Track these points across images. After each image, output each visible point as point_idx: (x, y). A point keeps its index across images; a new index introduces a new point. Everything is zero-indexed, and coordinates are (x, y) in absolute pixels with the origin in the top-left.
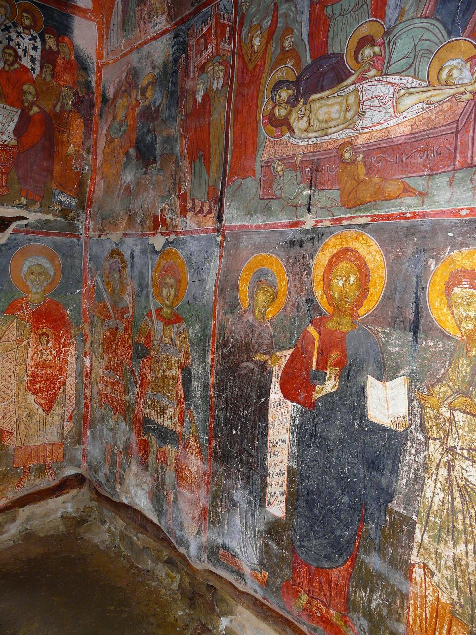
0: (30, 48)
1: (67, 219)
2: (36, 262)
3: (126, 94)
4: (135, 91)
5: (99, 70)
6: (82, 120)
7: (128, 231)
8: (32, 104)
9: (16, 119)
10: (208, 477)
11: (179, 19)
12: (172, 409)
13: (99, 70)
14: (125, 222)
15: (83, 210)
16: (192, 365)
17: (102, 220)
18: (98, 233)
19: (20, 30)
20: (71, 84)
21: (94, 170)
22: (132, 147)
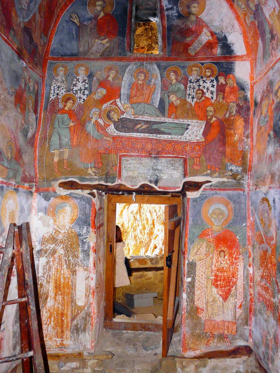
0: (210, 87)
1: (236, 180)
2: (217, 207)
3: (267, 98)
4: (271, 94)
5: (252, 88)
6: (243, 119)
7: (272, 186)
8: (212, 117)
9: (204, 127)
13: (252, 88)
14: (269, 179)
15: (246, 173)
17: (257, 179)
18: (255, 187)
19: (204, 79)
20: (234, 100)
21: (252, 148)
22: (271, 130)
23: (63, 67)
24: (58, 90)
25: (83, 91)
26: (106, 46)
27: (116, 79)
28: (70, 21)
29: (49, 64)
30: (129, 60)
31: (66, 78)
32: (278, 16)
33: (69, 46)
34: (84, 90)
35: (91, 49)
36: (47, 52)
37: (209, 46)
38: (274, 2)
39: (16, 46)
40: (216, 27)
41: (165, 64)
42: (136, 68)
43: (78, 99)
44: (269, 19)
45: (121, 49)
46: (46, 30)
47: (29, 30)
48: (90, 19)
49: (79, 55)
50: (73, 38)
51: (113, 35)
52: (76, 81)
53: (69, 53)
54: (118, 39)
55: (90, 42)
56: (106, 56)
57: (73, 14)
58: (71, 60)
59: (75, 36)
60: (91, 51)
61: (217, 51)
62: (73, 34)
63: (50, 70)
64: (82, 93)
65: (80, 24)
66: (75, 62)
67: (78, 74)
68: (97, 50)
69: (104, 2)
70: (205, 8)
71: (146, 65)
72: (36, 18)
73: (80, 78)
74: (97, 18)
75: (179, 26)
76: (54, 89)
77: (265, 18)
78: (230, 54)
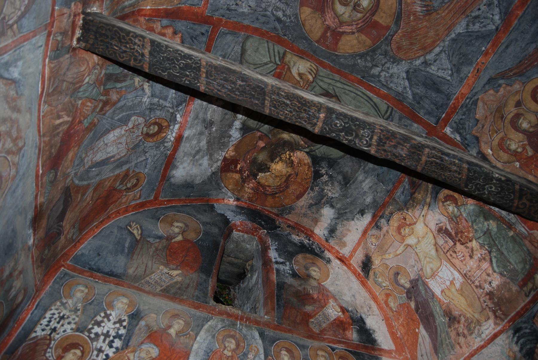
11: (512, 314)
23: (87, 287)
24: (58, 323)
25: (111, 338)
26: (175, 280)
27: (183, 336)
28: (126, 229)
29: (61, 274)
30: (211, 312)
31: (84, 307)
32: (462, 289)
33: (110, 259)
34: (115, 337)
35: (148, 276)
36: (66, 256)
37: (339, 325)
38: (451, 272)
39: (42, 200)
40: (347, 302)
41: (272, 334)
42: (223, 328)
43: (95, 353)
44: (440, 297)
45: (200, 291)
46: (84, 224)
47: (70, 199)
48: (160, 238)
49: (124, 278)
50: (122, 252)
51: (191, 268)
52: (104, 317)
53: (107, 270)
54: (199, 276)
55: (150, 265)
56: (171, 293)
57: (135, 223)
58: (106, 281)
59: (126, 251)
60: (147, 278)
61: (352, 335)
62: (124, 247)
63: (58, 283)
64: (107, 342)
65: (141, 238)
66: (112, 286)
67: (111, 306)
68: (158, 280)
69: (187, 226)
70: (328, 276)
71: (241, 327)
72: (86, 192)
73: (114, 315)
74: (171, 239)
75: (294, 287)
76: (51, 318)
77: (433, 295)
78: (372, 344)
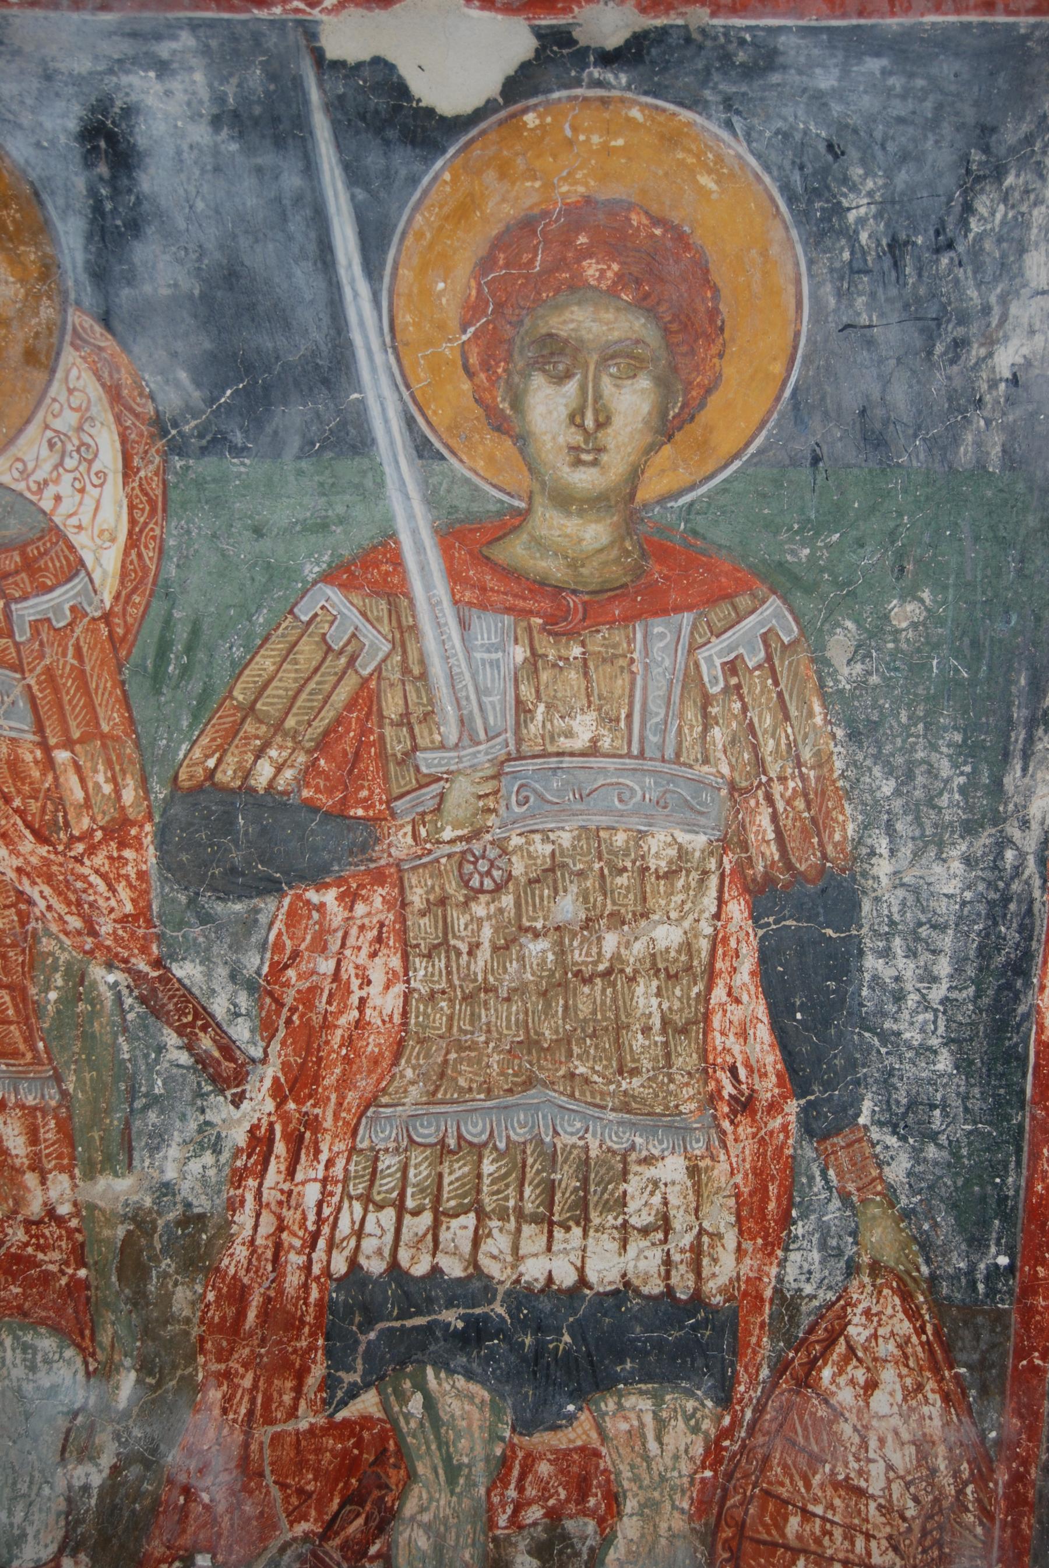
10: (1018, 1478)
12: (673, 1168)
16: (860, 855)
